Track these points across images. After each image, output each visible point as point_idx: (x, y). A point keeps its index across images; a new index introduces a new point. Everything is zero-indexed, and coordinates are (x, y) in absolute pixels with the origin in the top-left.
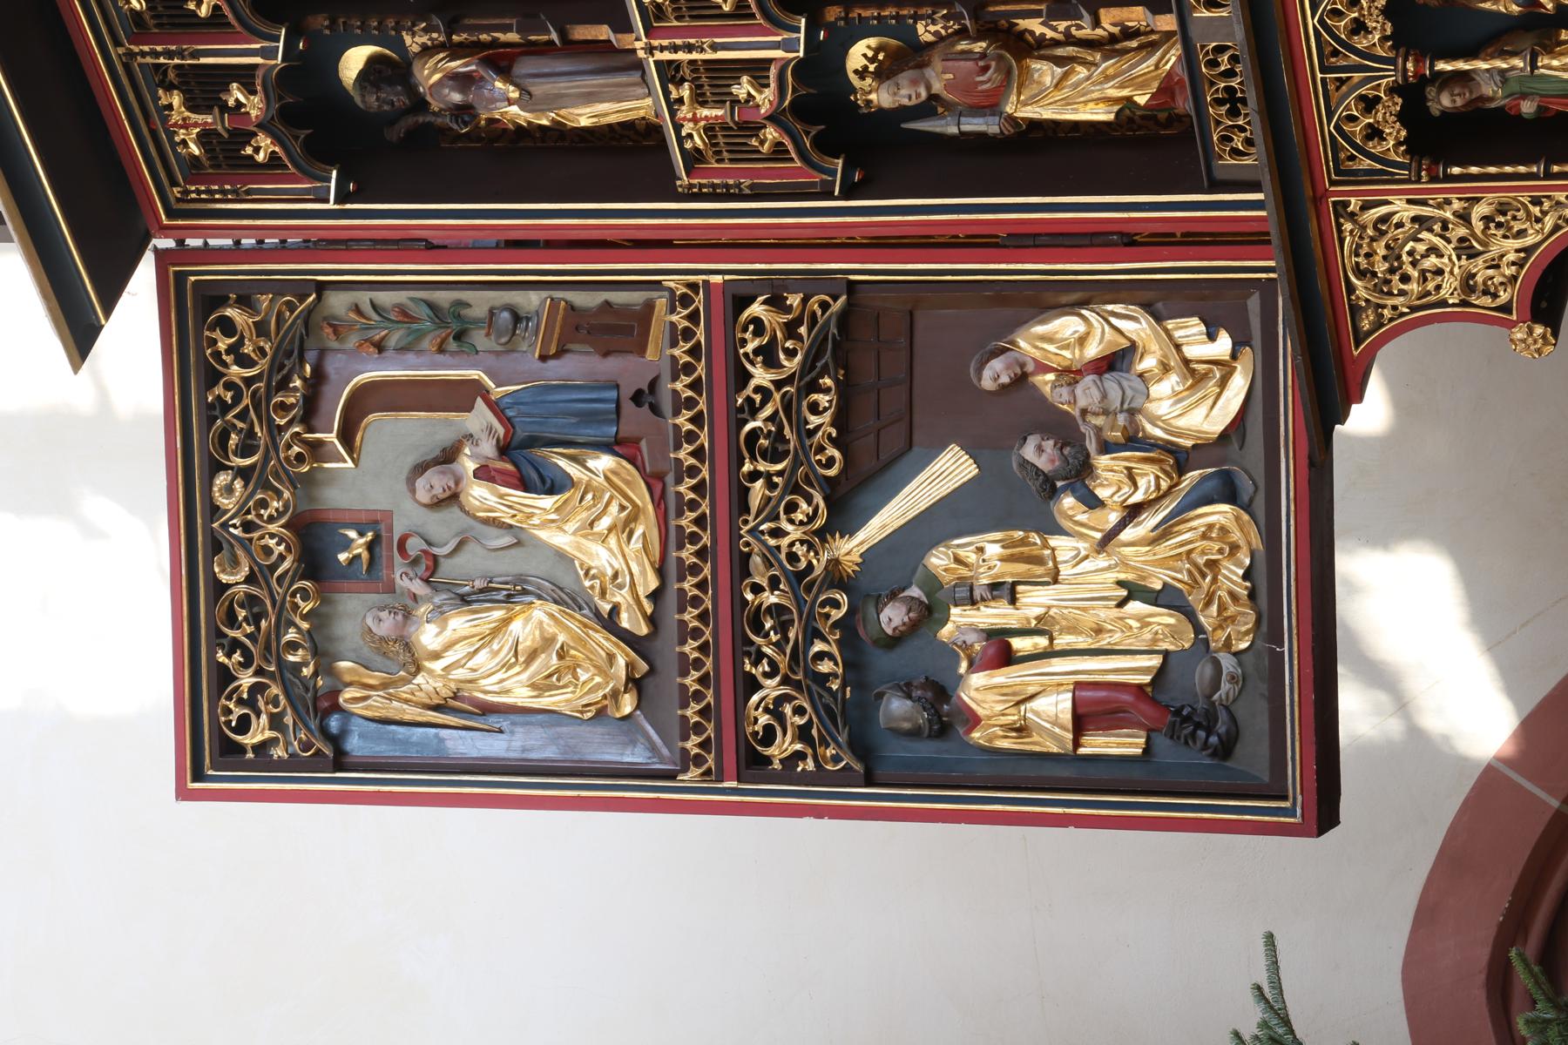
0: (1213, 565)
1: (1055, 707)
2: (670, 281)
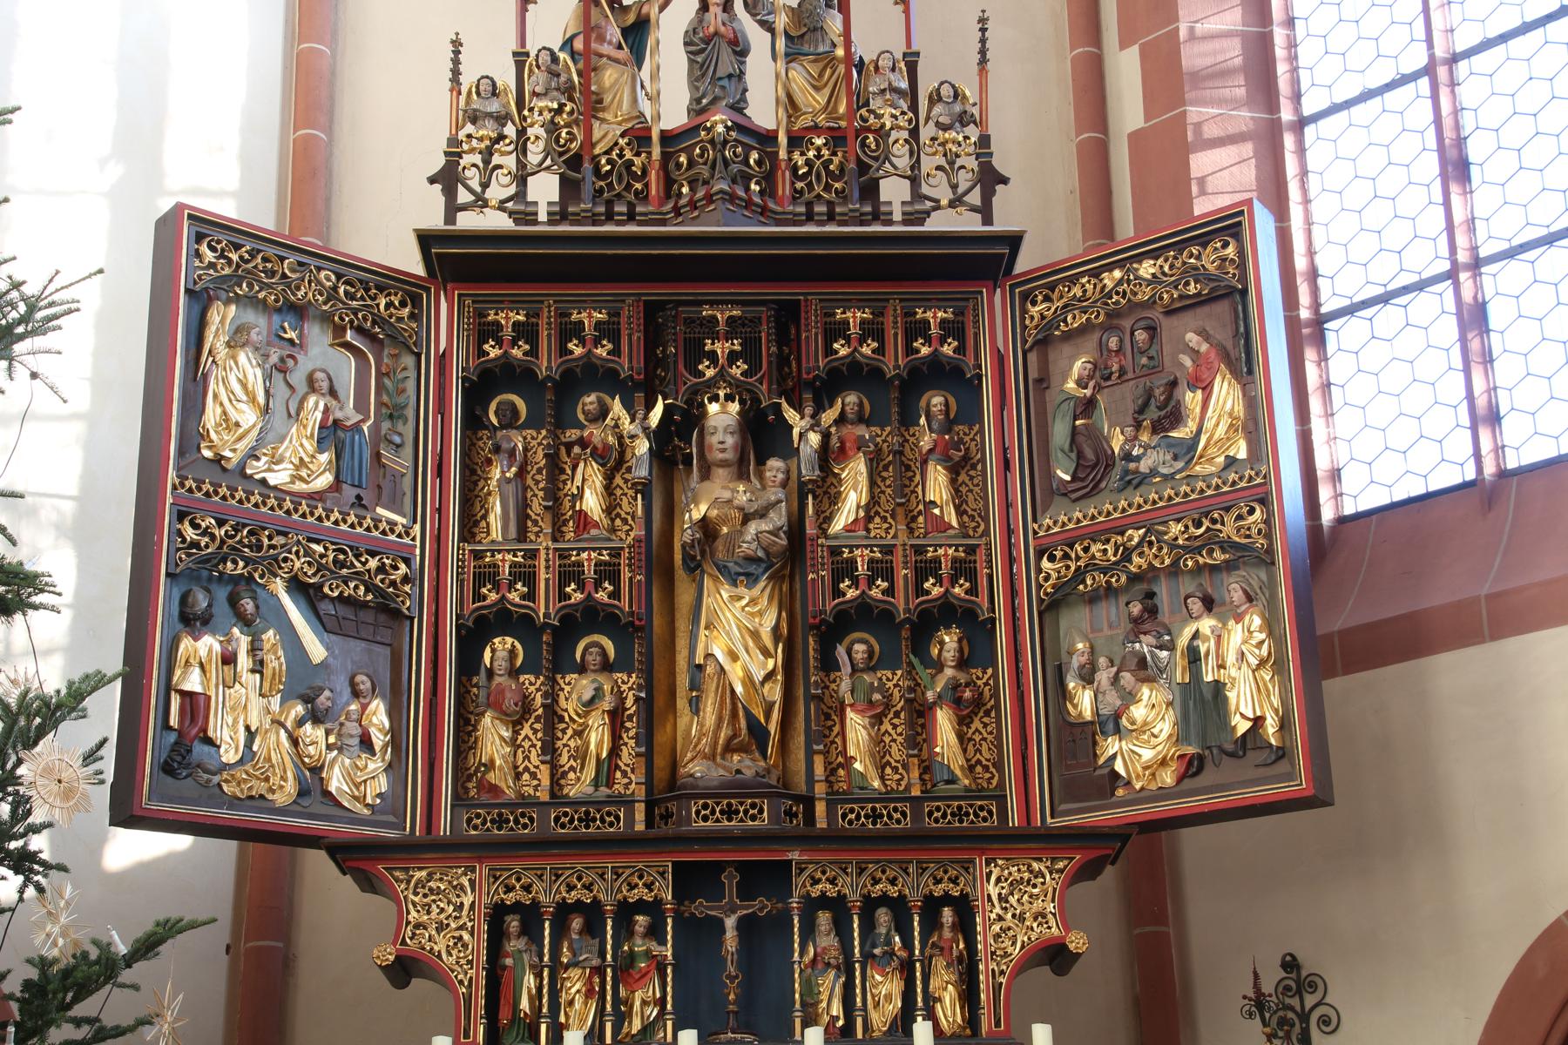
0: (267, 779)
1: (193, 683)
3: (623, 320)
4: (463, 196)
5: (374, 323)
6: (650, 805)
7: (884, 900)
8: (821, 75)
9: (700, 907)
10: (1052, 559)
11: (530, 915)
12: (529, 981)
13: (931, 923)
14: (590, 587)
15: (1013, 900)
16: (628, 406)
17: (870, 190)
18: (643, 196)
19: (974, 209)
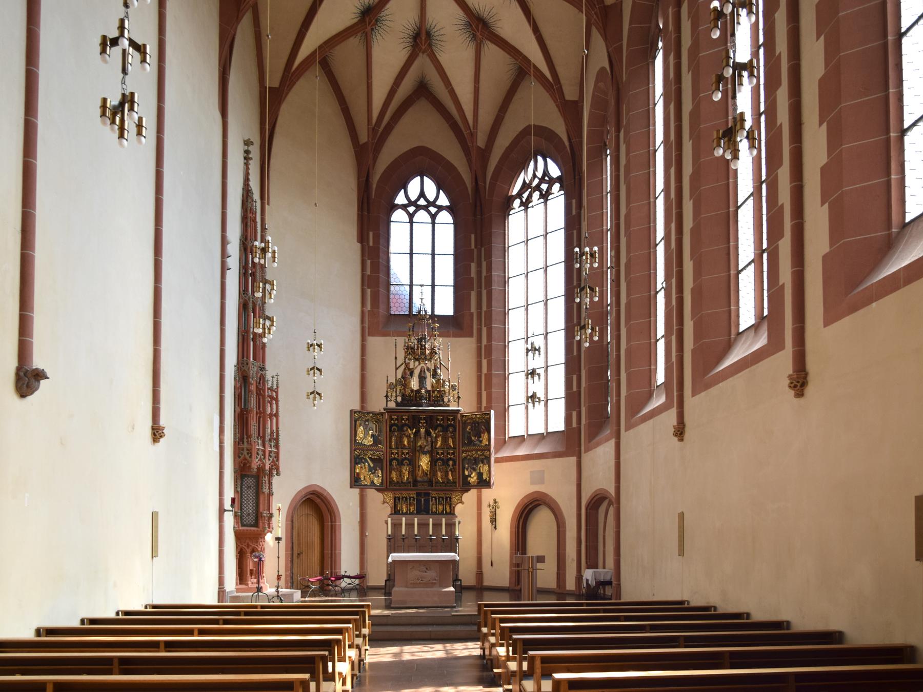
4: (389, 399)
6: (413, 483)
7: (441, 497)
9: (419, 497)
11: (399, 498)
12: (399, 505)
13: (446, 499)
17: (443, 400)
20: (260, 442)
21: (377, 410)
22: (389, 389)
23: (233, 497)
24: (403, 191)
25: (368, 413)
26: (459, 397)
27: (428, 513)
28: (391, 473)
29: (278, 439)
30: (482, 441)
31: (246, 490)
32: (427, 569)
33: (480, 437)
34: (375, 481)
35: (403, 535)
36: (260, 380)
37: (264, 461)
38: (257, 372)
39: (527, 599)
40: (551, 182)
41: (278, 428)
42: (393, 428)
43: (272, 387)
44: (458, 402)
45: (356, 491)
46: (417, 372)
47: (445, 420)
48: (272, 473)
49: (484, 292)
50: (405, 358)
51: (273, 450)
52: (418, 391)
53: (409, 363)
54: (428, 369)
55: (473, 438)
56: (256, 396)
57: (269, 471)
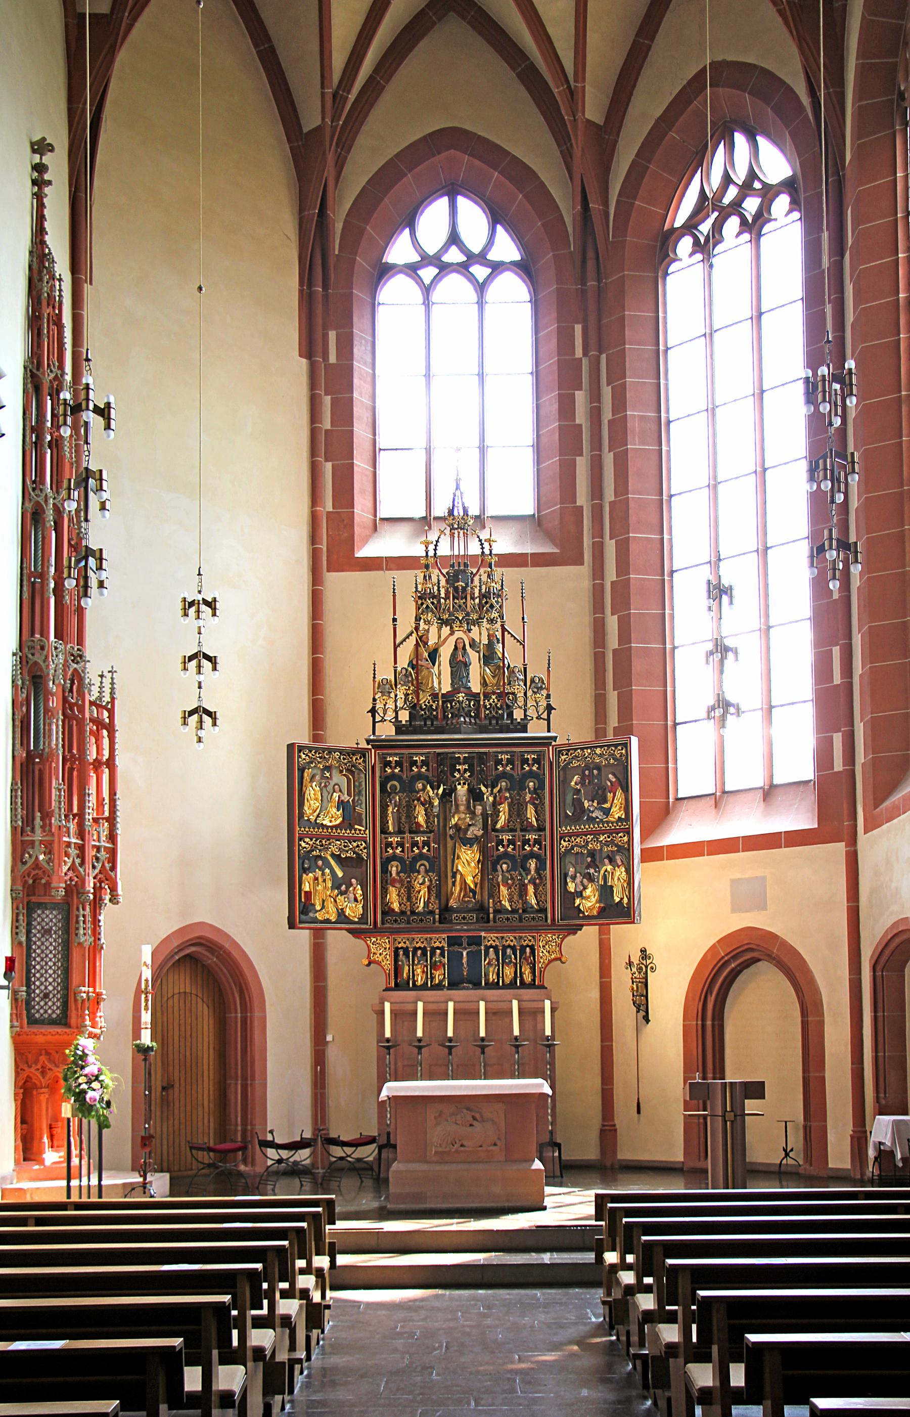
2: (368, 831)
3: (430, 759)
4: (378, 718)
5: (352, 766)
8: (495, 671)
10: (564, 841)
14: (421, 848)
15: (547, 947)
16: (433, 790)
17: (510, 715)
18: (436, 717)
19: (544, 719)
20: (73, 826)
21: (350, 744)
22: (379, 695)
23: (9, 955)
24: (407, 231)
25: (330, 751)
26: (549, 708)
27: (477, 985)
28: (385, 891)
29: (115, 819)
30: (610, 809)
31: (39, 939)
32: (474, 1118)
33: (605, 801)
34: (348, 912)
35: (420, 1040)
36: (72, 684)
37: (81, 870)
38: (66, 665)
39: (722, 1186)
40: (769, 193)
41: (115, 795)
42: (389, 786)
43: (100, 698)
44: (548, 720)
45: (304, 936)
46: (445, 653)
47: (518, 763)
48: (101, 899)
49: (608, 459)
50: (418, 619)
51: (103, 844)
52: (448, 697)
53: (428, 631)
54: (473, 644)
55: (586, 804)
56: (63, 721)
57: (94, 894)
